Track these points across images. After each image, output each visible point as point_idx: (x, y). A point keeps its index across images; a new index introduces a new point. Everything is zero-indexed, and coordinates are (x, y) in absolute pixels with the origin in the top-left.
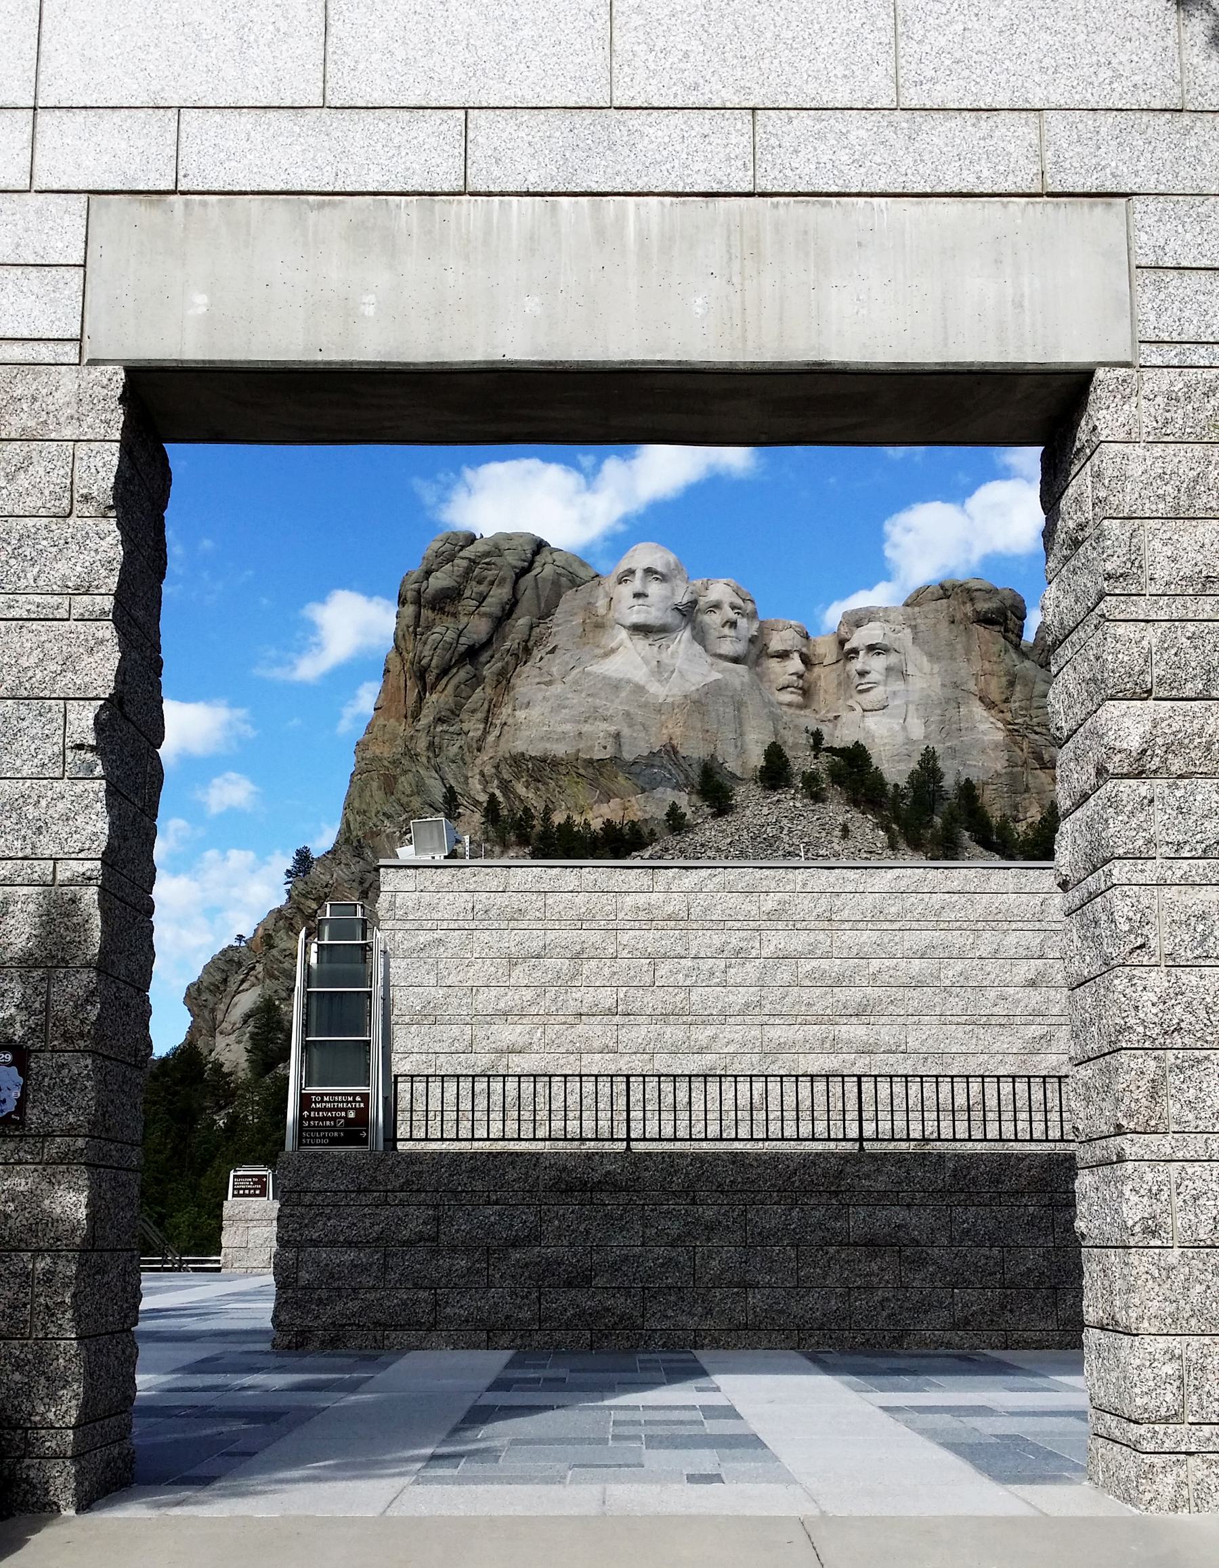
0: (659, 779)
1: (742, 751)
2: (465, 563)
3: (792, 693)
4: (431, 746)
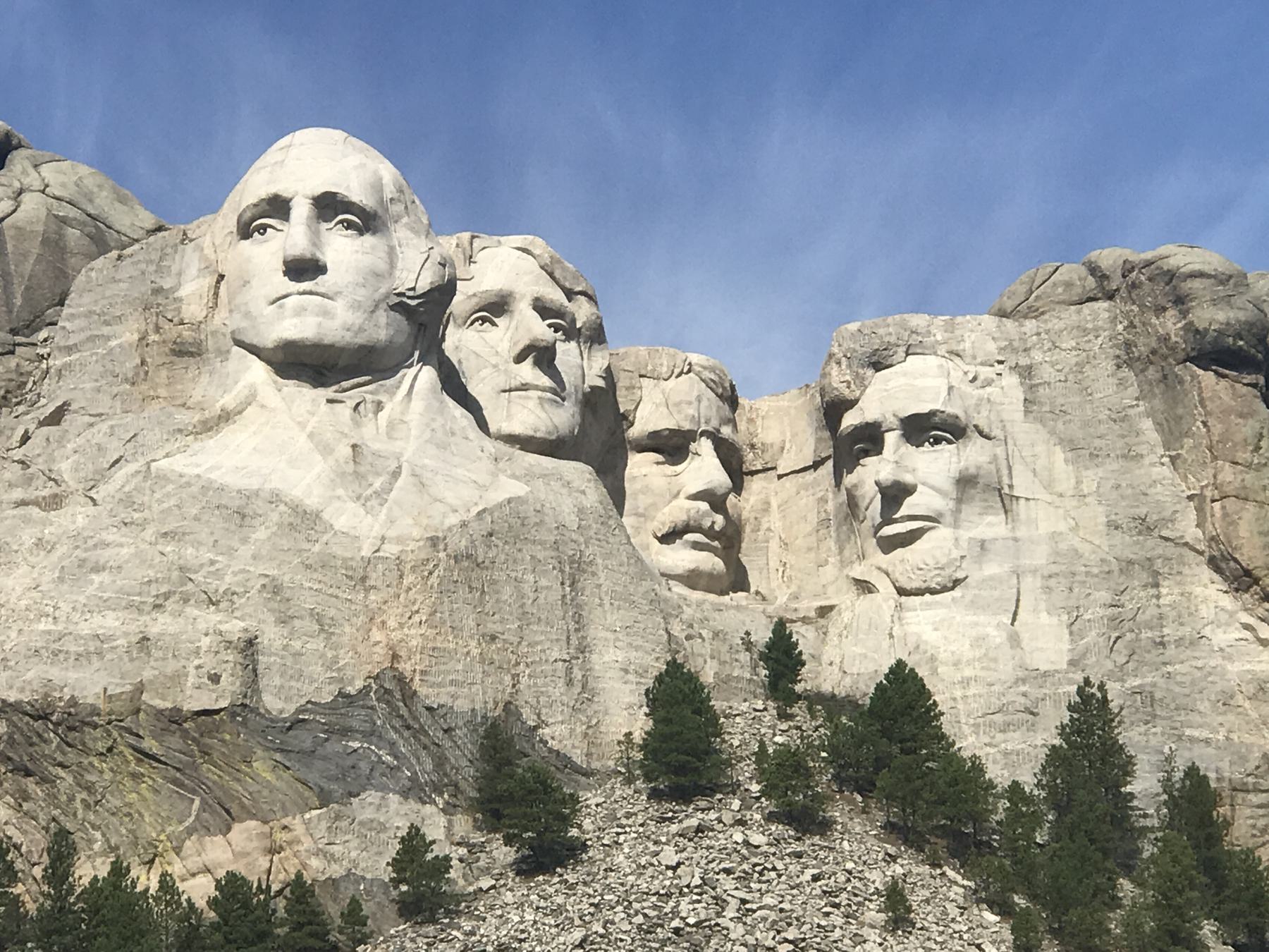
0: (364, 767)
1: (586, 692)
3: (696, 546)
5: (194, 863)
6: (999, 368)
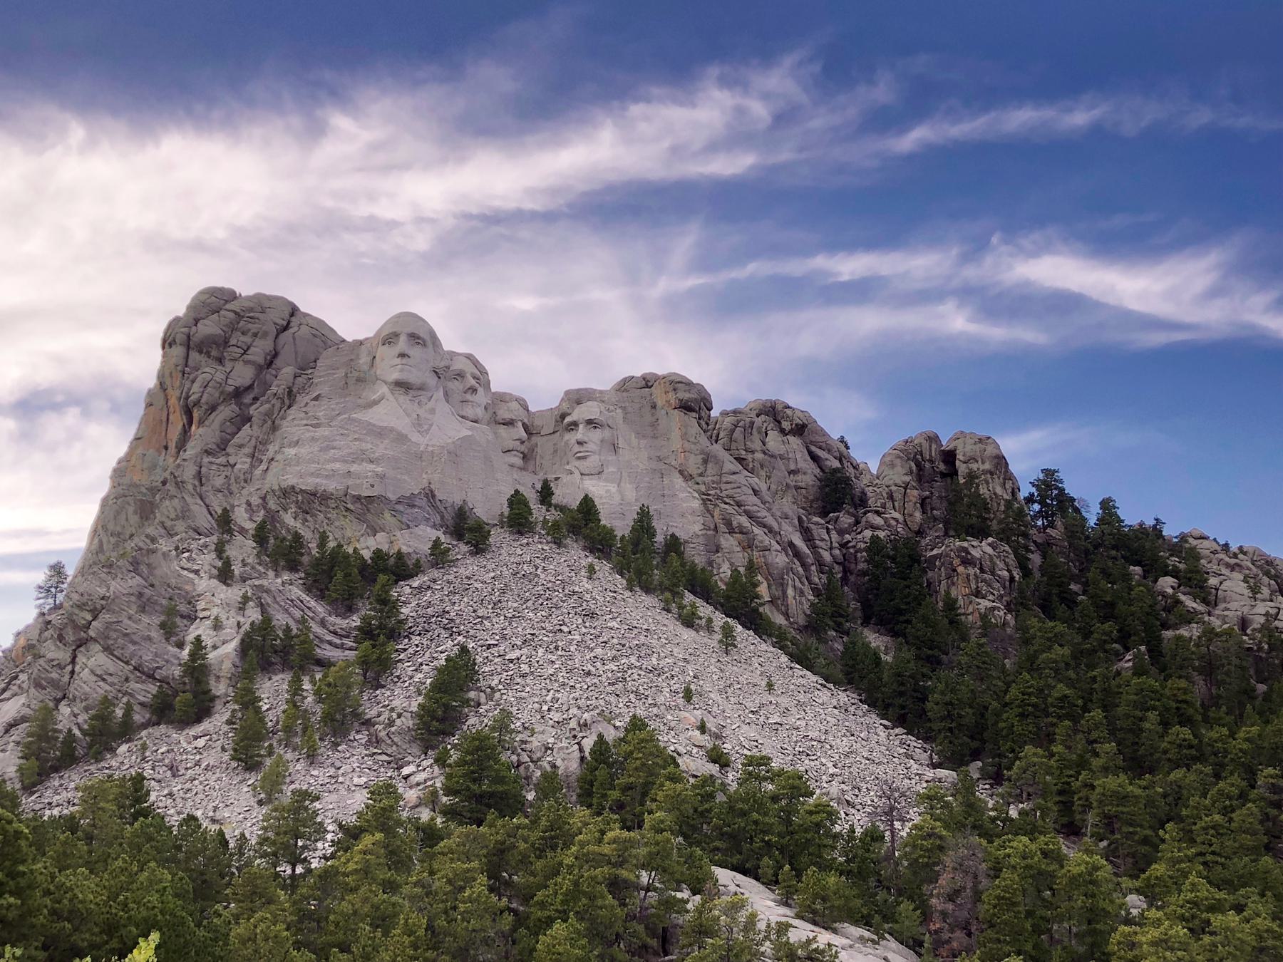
4: (199, 476)
5: (363, 545)
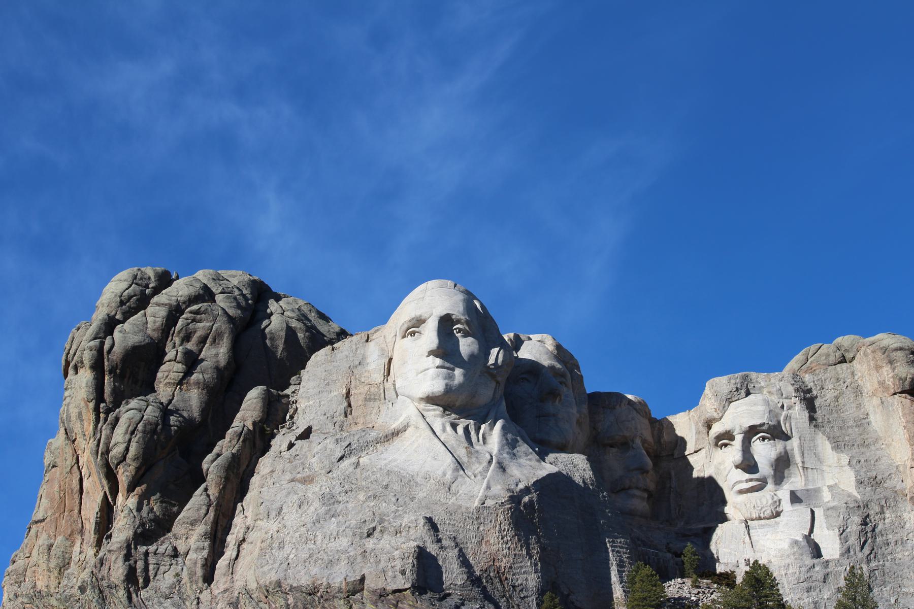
2: (162, 312)
3: (634, 496)
6: (794, 400)
